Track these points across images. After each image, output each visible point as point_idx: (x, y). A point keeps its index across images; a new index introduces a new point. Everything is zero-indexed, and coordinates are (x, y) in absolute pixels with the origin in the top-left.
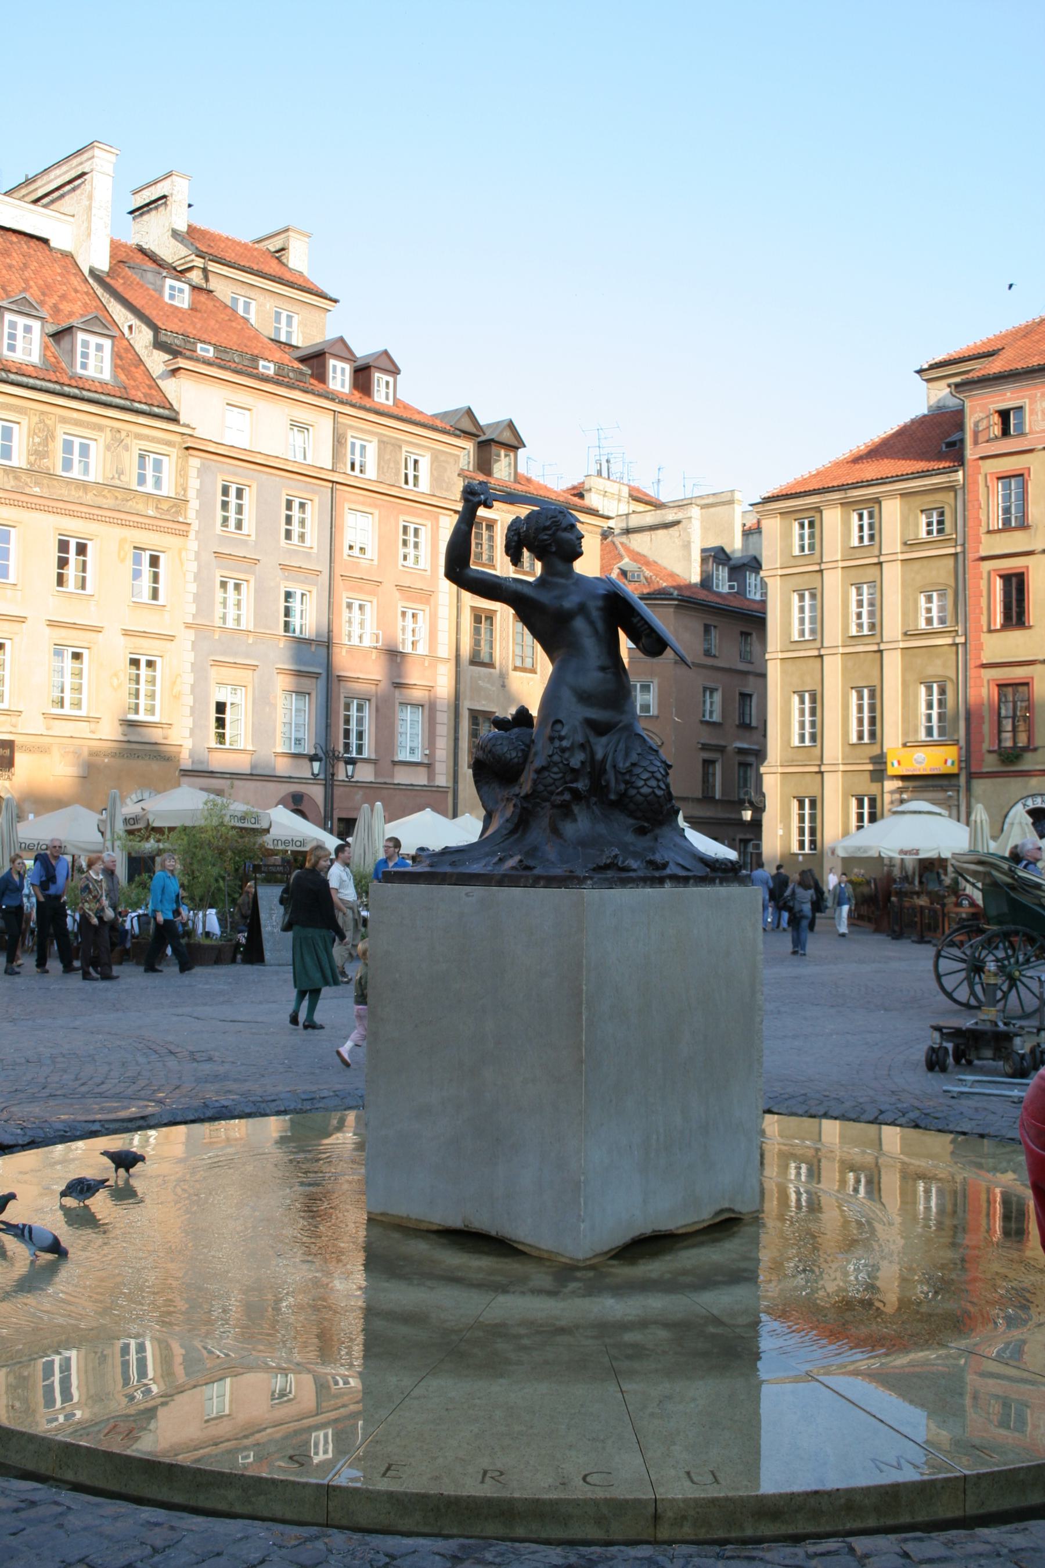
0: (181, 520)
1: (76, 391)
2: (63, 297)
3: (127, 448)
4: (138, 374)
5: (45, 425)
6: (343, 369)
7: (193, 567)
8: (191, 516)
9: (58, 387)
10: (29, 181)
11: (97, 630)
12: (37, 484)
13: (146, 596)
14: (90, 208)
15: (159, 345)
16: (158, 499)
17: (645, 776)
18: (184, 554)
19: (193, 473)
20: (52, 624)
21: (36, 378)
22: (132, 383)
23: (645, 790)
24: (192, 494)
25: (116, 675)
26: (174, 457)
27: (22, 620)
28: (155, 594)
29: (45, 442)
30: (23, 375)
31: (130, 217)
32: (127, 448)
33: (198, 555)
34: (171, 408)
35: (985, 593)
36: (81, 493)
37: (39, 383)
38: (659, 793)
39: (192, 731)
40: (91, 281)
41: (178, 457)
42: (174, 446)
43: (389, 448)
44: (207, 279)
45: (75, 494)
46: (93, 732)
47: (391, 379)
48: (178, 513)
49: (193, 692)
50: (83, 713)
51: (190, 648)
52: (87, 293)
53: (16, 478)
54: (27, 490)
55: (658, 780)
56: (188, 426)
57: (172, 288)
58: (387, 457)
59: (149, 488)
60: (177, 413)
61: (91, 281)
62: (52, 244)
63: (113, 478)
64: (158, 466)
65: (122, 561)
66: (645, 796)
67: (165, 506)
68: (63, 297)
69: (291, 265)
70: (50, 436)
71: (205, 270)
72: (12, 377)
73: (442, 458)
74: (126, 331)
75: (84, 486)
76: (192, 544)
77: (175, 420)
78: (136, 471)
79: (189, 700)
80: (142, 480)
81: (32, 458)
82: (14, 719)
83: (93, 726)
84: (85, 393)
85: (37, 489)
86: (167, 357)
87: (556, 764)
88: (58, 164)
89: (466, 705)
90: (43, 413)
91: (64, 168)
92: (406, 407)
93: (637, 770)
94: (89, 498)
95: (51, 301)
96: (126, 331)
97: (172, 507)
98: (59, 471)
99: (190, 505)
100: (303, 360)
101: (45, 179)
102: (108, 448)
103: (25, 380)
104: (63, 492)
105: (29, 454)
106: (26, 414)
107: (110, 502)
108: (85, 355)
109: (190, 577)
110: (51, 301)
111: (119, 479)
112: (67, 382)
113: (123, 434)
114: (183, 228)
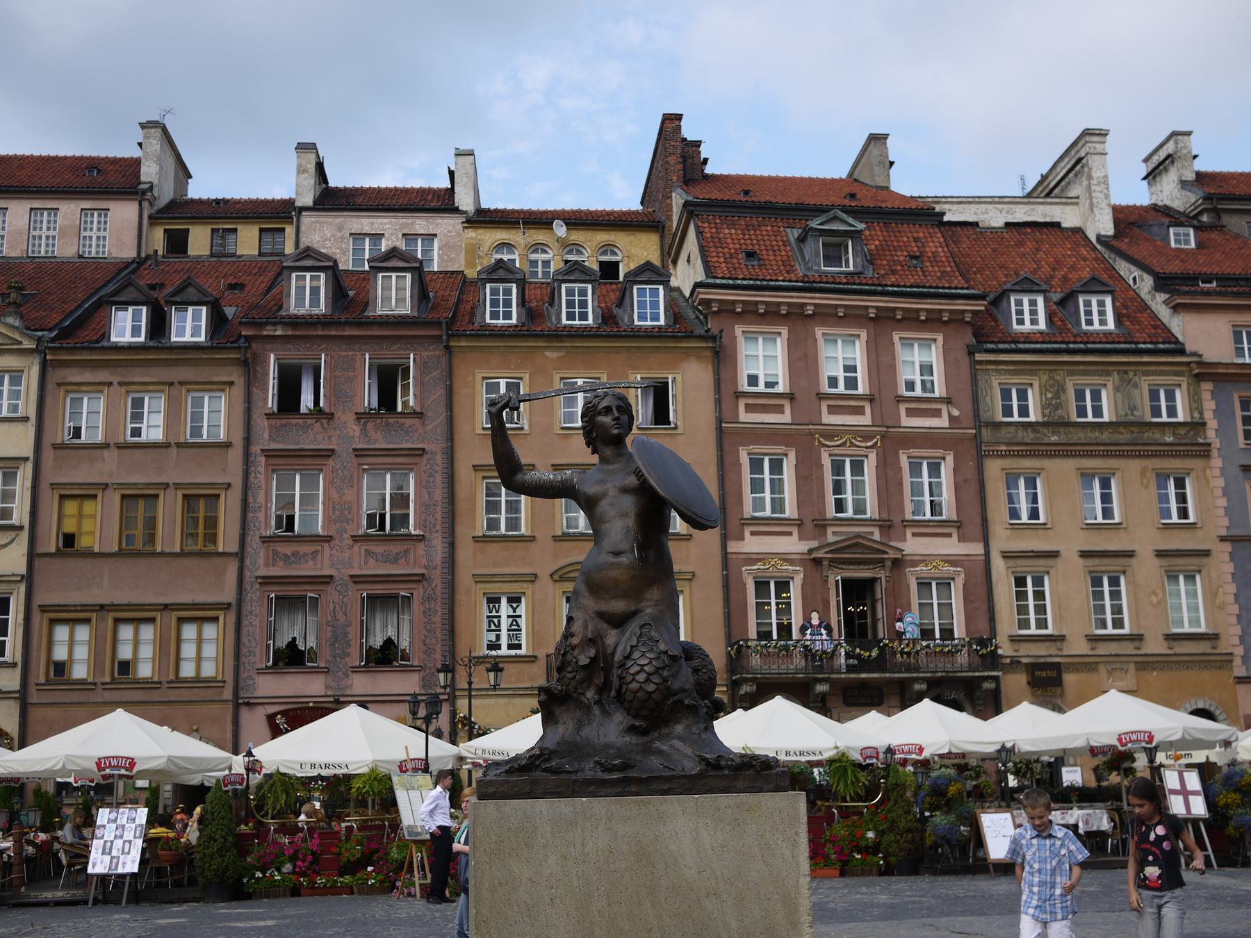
0: (1201, 441)
1: (1082, 346)
2: (1073, 268)
3: (1136, 386)
4: (1143, 318)
5: (1055, 381)
7: (1220, 482)
8: (1211, 434)
9: (1063, 346)
10: (1044, 178)
11: (1130, 554)
12: (1054, 433)
13: (1175, 519)
14: (1089, 186)
17: (632, 671)
18: (1208, 472)
19: (1206, 396)
20: (1085, 554)
21: (1043, 342)
23: (634, 686)
24: (1208, 416)
25: (1154, 593)
26: (1185, 386)
27: (1054, 555)
28: (1183, 513)
29: (1057, 395)
30: (1031, 342)
31: (1145, 182)
32: (1136, 386)
34: (1177, 341)
37: (1045, 346)
38: (651, 688)
39: (1242, 638)
40: (1099, 247)
41: (1189, 384)
44: (1220, 218)
48: (1197, 435)
49: (1237, 601)
50: (1126, 631)
51: (1228, 559)
52: (1096, 259)
53: (1034, 431)
54: (1046, 440)
55: (649, 674)
59: (1165, 418)
61: (1099, 247)
62: (1064, 225)
64: (1170, 397)
65: (1146, 487)
68: (1073, 268)
70: (1061, 389)
72: (1021, 346)
74: (1131, 283)
77: (1182, 352)
78: (1147, 404)
79: (1235, 609)
80: (1156, 412)
81: (1047, 412)
82: (1059, 644)
83: (1137, 643)
84: (1089, 346)
86: (1167, 296)
88: (1061, 158)
90: (1051, 371)
91: (1066, 160)
93: (630, 663)
94: (1105, 436)
95: (1059, 274)
96: (1131, 283)
98: (1074, 418)
101: (1054, 173)
103: (1033, 346)
104: (1079, 436)
105: (1043, 408)
107: (1125, 436)
108: (1088, 313)
109: (1219, 492)
110: (1059, 274)
112: (1072, 339)
113: (1131, 374)
114: (1191, 176)
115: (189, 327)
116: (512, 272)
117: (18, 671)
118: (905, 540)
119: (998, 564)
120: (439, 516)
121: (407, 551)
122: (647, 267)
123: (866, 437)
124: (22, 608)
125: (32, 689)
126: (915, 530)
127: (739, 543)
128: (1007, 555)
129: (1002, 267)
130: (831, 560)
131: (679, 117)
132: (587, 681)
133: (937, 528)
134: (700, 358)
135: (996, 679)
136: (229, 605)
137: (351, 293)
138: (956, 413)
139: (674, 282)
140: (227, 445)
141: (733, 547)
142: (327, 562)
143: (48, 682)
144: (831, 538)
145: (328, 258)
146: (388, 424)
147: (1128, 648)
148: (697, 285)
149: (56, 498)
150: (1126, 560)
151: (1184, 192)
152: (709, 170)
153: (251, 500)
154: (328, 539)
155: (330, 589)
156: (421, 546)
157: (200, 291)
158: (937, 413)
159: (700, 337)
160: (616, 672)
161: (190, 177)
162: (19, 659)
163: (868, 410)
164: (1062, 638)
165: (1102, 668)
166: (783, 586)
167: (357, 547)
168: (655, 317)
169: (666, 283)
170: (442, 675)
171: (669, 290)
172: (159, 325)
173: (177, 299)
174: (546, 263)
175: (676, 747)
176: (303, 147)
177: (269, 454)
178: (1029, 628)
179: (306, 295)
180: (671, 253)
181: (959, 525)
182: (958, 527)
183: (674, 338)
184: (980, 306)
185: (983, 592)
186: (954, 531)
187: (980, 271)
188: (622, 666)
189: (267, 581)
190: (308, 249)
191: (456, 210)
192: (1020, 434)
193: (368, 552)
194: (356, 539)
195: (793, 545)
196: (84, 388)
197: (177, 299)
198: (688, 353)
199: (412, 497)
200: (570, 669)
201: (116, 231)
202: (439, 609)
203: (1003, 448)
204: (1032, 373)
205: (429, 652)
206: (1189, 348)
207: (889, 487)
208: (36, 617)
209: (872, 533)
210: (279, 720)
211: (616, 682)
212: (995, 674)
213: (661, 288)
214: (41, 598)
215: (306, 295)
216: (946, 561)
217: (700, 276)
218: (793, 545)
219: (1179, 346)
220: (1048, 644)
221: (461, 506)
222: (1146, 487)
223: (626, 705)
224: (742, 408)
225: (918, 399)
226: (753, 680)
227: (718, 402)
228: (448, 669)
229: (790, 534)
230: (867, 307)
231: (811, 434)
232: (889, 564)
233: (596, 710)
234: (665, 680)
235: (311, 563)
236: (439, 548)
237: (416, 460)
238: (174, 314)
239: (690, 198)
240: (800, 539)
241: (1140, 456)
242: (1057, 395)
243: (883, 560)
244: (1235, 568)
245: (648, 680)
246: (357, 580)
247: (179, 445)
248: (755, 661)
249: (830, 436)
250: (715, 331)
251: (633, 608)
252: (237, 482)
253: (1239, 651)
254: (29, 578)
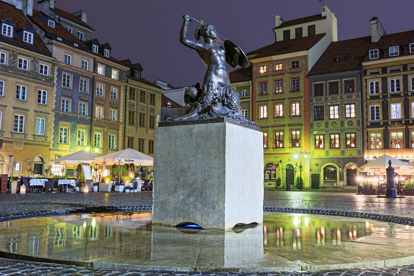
5: (15, 55)
6: (96, 47)
7: (55, 95)
8: (55, 82)
15: (46, 36)
16: (46, 77)
19: (56, 70)
20: (14, 108)
22: (39, 45)
24: (55, 76)
25: (32, 123)
27: (6, 106)
33: (56, 92)
35: (257, 111)
36: (24, 73)
42: (51, 63)
43: (108, 68)
44: (59, 22)
46: (25, 138)
47: (109, 51)
48: (51, 81)
49: (54, 129)
53: (5, 68)
56: (55, 58)
57: (50, 22)
58: (108, 70)
59: (43, 74)
60: (52, 54)
62: (17, 7)
63: (33, 70)
65: (35, 92)
67: (48, 79)
68: (19, 22)
69: (82, 20)
71: (59, 19)
73: (122, 72)
75: (25, 72)
76: (55, 90)
77: (51, 55)
78: (40, 69)
80: (41, 72)
81: (10, 63)
87: (211, 94)
89: (127, 134)
90: (13, 51)
92: (113, 58)
97: (50, 79)
99: (55, 79)
100: (85, 44)
102: (32, 62)
105: (9, 61)
106: (8, 51)
109: (54, 98)
111: (35, 70)
113: (36, 59)
151: (50, 11)
206: (53, 56)
219: (50, 55)
222: (35, 92)
241: (35, 82)
242: (14, 59)
244: (55, 119)
253: (52, 142)
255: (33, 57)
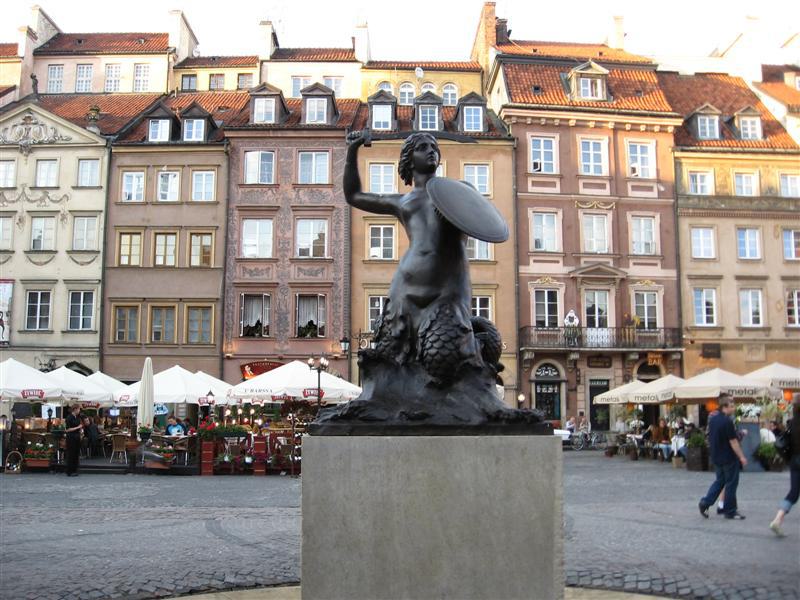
9: (729, 149)
11: (765, 278)
12: (724, 203)
23: (433, 351)
27: (719, 278)
32: (773, 174)
38: (446, 352)
45: (745, 204)
54: (717, 207)
55: (444, 342)
66: (433, 356)
68: (736, 101)
82: (720, 332)
85: (723, 206)
87: (385, 334)
93: (429, 334)
103: (710, 148)
104: (738, 204)
107: (765, 204)
110: (728, 105)
115: (195, 131)
116: (389, 98)
117: (98, 335)
118: (628, 267)
119: (686, 284)
120: (342, 248)
121: (323, 269)
122: (472, 95)
123: (606, 204)
124: (99, 299)
125: (106, 347)
126: (635, 261)
127: (527, 267)
128: (690, 277)
129: (693, 100)
130: (583, 278)
131: (494, 4)
132: (397, 349)
133: (646, 260)
134: (504, 152)
135: (681, 352)
136: (217, 299)
137: (291, 112)
138: (662, 189)
139: (489, 106)
140: (216, 203)
141: (523, 269)
142: (275, 276)
143: (115, 343)
144: (583, 265)
145: (277, 90)
146: (312, 191)
147: (761, 336)
148: (504, 107)
149: (118, 235)
150: (763, 282)
152: (512, 38)
153: (230, 236)
154: (275, 260)
155: (277, 290)
156: (332, 266)
157: (201, 109)
158: (650, 189)
159: (505, 139)
160: (421, 340)
161: (197, 43)
162: (98, 329)
163: (608, 186)
164: (722, 329)
165: (745, 349)
166: (552, 296)
167: (293, 266)
168: (477, 126)
169: (484, 106)
170: (343, 344)
171: (487, 111)
172: (176, 131)
173: (188, 115)
174: (411, 94)
175: (463, 401)
176: (264, 23)
177: (241, 209)
178: (702, 322)
179: (264, 112)
180: (487, 85)
181: (662, 258)
182: (662, 260)
183: (489, 139)
184: (679, 122)
185: (674, 302)
186: (659, 262)
187: (679, 102)
188: (424, 336)
189: (238, 285)
190: (265, 84)
191: (356, 61)
192: (702, 203)
193: (299, 269)
194: (292, 260)
195: (560, 269)
196: (134, 169)
197: (188, 115)
198: (496, 151)
199: (326, 235)
200: (385, 339)
201: (152, 77)
202: (341, 304)
203: (691, 211)
204: (710, 165)
205: (336, 330)
207: (620, 233)
208: (107, 303)
209: (608, 263)
210: (247, 369)
211: (420, 349)
212: (679, 349)
213: (481, 108)
214: (110, 294)
215: (264, 112)
216: (653, 281)
217: (505, 100)
218: (560, 269)
220: (713, 332)
221: (356, 242)
223: (427, 365)
224: (530, 184)
225: (640, 180)
226: (532, 351)
227: (516, 181)
228: (345, 340)
229: (558, 262)
230: (607, 122)
231: (572, 201)
232: (618, 281)
233: (403, 371)
234: (457, 347)
235: (265, 276)
236: (342, 267)
237: (328, 213)
238: (186, 124)
239: (500, 53)
240: (565, 265)
241: (774, 218)
243: (614, 279)
245: (443, 347)
246: (293, 285)
247: (188, 203)
248: (534, 339)
249: (584, 203)
250: (513, 135)
251: (434, 293)
252: (222, 225)
254: (103, 281)
255: (763, 166)
